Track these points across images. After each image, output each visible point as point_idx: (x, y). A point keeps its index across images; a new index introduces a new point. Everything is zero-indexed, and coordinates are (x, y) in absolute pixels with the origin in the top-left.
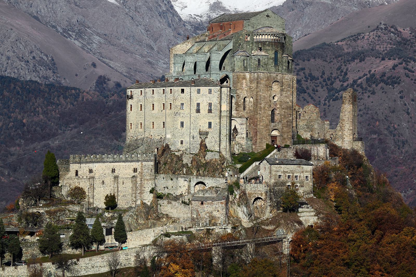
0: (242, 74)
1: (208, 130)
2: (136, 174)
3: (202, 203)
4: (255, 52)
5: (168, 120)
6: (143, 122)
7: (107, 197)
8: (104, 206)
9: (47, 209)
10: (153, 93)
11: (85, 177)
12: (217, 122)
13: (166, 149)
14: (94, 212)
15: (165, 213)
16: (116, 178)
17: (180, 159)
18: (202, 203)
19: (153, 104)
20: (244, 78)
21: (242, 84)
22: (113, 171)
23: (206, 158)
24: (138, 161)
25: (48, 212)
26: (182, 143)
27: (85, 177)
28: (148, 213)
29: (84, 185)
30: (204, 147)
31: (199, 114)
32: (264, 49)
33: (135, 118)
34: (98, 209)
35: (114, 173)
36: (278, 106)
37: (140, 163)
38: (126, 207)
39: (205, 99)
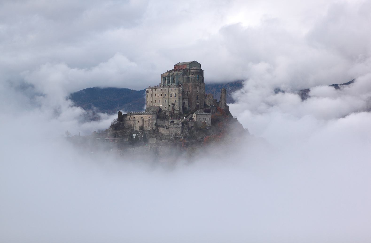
0: (186, 83)
1: (174, 103)
2: (150, 119)
3: (173, 128)
4: (191, 76)
7: (140, 127)
8: (139, 130)
9: (119, 131)
10: (155, 91)
11: (132, 120)
13: (160, 110)
14: (136, 132)
15: (160, 132)
17: (165, 113)
18: (173, 128)
20: (187, 85)
21: (186, 87)
22: (142, 118)
24: (150, 114)
25: (120, 132)
26: (166, 107)
28: (154, 133)
29: (132, 123)
30: (174, 109)
34: (137, 131)
36: (199, 94)
37: (151, 115)
38: (146, 130)
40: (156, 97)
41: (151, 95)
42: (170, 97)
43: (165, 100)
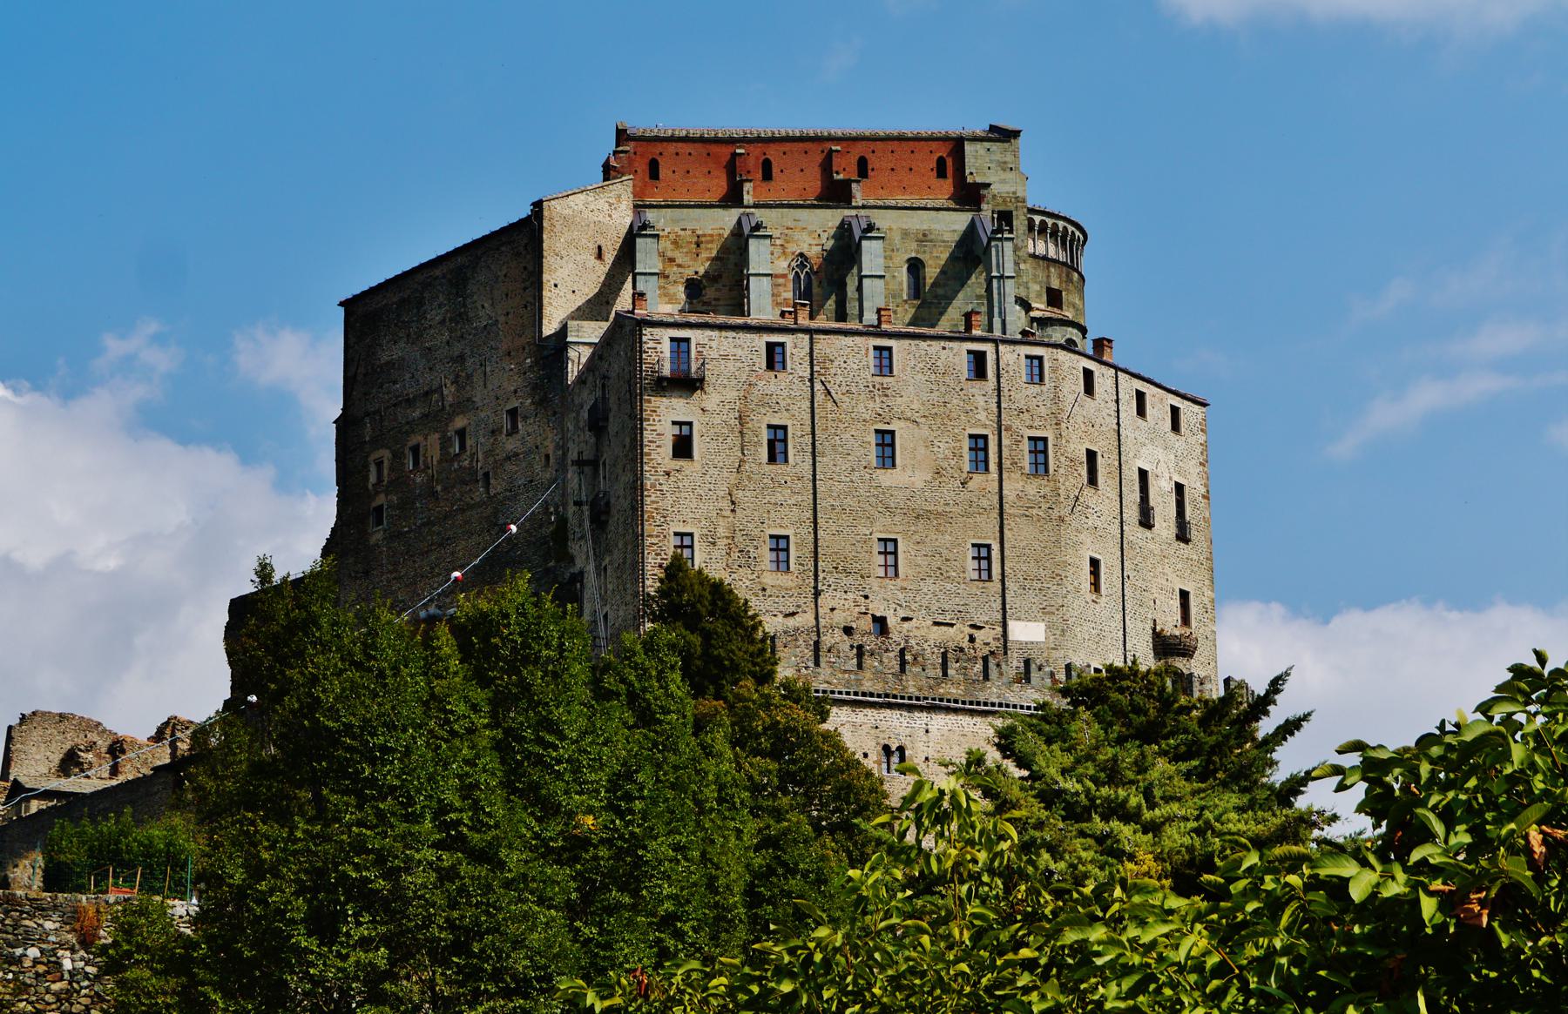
5: (1020, 534)
31: (1148, 533)
33: (726, 504)
40: (908, 476)
42: (1132, 514)
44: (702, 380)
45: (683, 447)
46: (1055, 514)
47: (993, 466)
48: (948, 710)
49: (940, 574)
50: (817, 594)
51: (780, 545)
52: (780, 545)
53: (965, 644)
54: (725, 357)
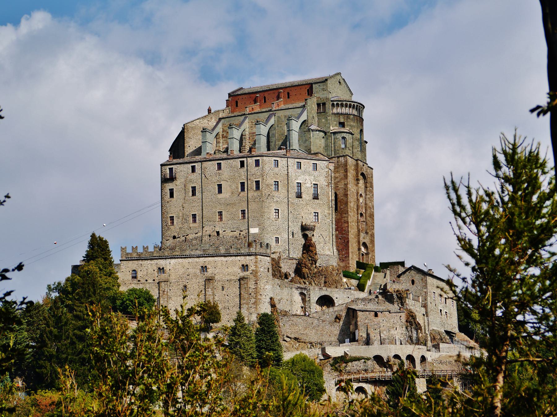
3: (376, 315)
5: (253, 206)
6: (198, 213)
11: (150, 281)
12: (326, 214)
15: (293, 336)
16: (209, 280)
18: (376, 315)
19: (220, 186)
22: (204, 269)
23: (318, 265)
26: (277, 240)
27: (150, 281)
31: (300, 199)
32: (348, 125)
33: (181, 208)
35: (206, 273)
36: (364, 211)
37: (252, 257)
39: (307, 177)
40: (226, 194)
41: (194, 189)
42: (293, 195)
43: (274, 206)
44: (175, 178)
45: (172, 195)
46: (261, 200)
47: (246, 190)
48: (175, 258)
49: (233, 219)
50: (203, 227)
51: (194, 216)
52: (194, 216)
53: (238, 236)
54: (181, 171)
